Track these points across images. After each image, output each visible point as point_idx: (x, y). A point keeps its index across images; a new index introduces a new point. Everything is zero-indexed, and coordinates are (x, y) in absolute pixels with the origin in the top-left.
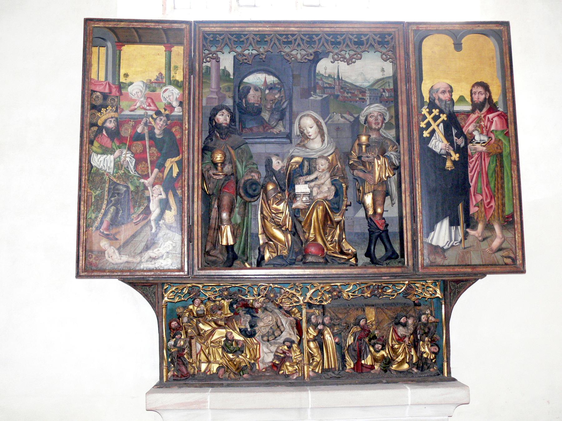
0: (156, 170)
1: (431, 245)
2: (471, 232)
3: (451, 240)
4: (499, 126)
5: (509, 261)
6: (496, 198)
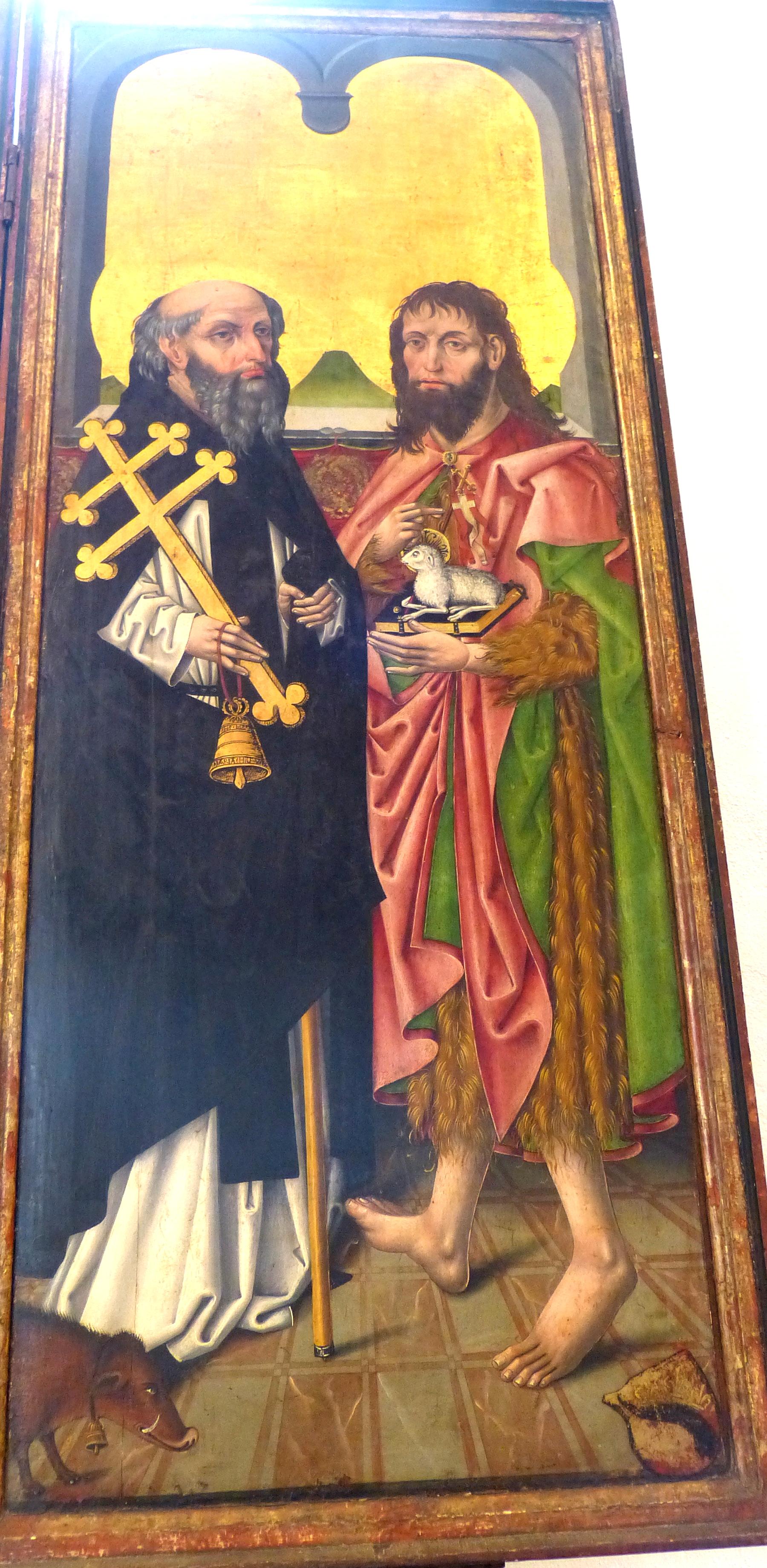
1: (71, 1329)
2: (386, 1225)
3: (227, 1289)
5: (669, 1443)
6: (558, 973)
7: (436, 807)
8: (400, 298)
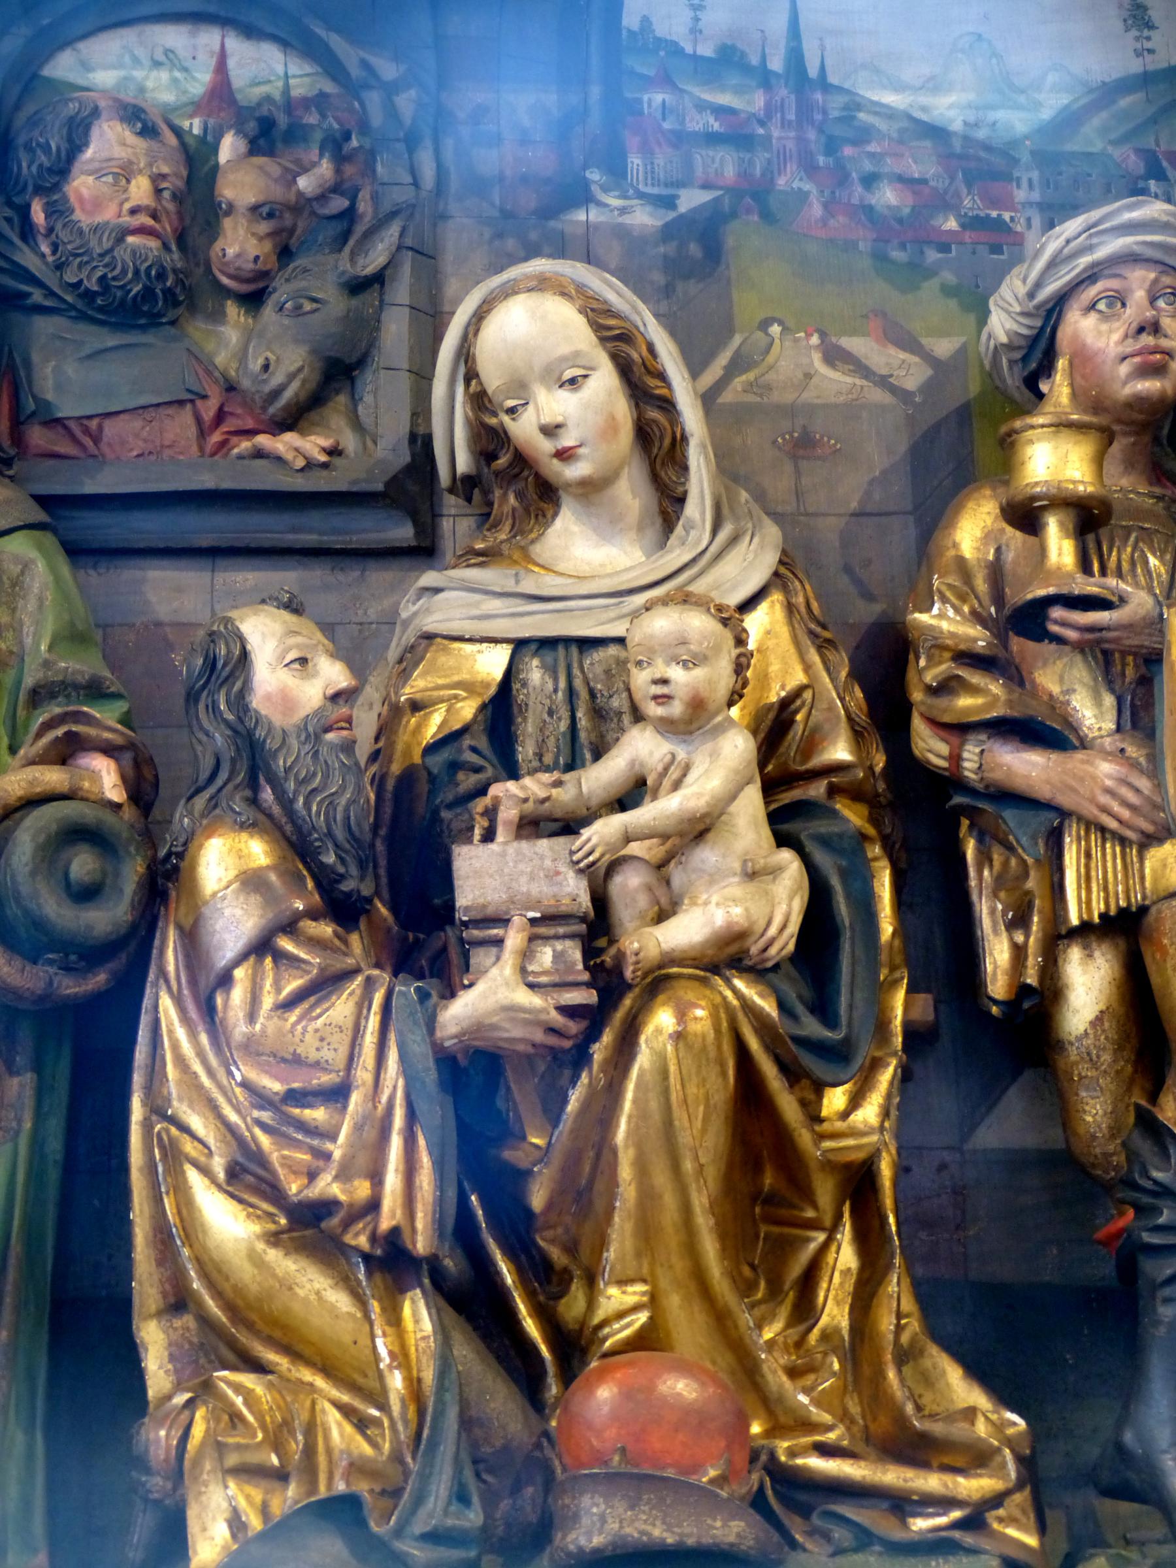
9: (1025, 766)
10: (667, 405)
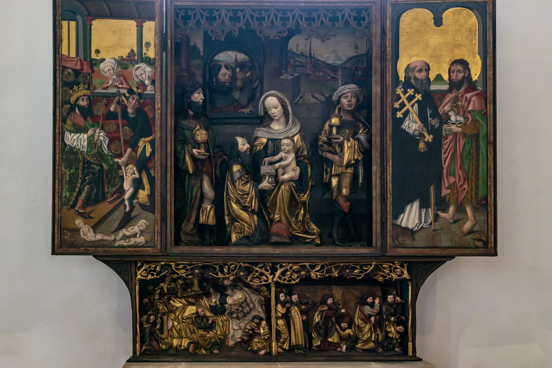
0: (129, 150)
1: (400, 226)
2: (442, 215)
3: (421, 222)
4: (477, 105)
5: (480, 244)
7: (452, 155)
8: (450, 63)
9: (329, 156)
10: (288, 110)
